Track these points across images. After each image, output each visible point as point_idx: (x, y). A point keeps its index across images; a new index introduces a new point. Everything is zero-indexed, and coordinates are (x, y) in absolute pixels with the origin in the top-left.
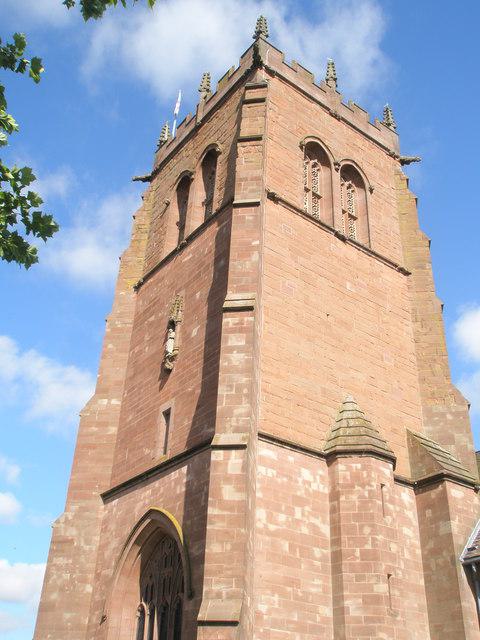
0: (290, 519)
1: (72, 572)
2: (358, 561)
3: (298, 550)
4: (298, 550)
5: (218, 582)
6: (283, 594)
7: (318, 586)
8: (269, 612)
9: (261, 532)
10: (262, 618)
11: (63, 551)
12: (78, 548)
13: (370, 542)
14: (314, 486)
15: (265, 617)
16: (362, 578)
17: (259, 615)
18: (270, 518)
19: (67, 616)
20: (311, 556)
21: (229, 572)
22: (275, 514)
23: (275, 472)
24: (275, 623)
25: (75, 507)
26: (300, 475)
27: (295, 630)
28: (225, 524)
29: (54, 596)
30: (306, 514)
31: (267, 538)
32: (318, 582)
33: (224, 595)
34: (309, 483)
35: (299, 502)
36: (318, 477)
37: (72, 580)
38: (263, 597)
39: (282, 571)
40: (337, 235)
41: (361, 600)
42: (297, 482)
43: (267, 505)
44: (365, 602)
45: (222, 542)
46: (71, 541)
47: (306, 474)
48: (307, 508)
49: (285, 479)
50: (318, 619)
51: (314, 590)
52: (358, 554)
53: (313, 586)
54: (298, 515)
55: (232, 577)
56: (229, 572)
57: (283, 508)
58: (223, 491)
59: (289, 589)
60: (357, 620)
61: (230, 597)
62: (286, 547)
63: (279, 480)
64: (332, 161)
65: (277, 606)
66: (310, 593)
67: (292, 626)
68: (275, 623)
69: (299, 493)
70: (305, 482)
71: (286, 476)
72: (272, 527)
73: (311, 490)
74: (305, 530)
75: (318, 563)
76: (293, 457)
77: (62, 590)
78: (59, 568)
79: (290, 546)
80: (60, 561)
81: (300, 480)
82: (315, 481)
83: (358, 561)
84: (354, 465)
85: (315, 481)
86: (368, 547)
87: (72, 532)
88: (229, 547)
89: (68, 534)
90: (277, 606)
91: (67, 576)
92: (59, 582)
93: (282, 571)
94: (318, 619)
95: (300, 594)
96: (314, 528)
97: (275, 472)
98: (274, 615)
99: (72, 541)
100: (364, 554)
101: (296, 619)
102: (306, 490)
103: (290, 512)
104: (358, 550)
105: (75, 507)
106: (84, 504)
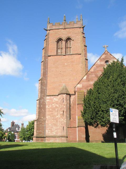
8: (48, 118)
9: (47, 108)
18: (48, 106)
24: (49, 119)
34: (55, 100)
35: (54, 103)
39: (50, 113)
40: (63, 55)
43: (48, 105)
47: (55, 99)
48: (55, 104)
50: (56, 118)
54: (53, 105)
59: (51, 115)
64: (63, 40)
68: (49, 119)
70: (54, 100)
72: (49, 108)
74: (54, 107)
76: (52, 97)
96: (56, 106)
98: (49, 118)
103: (52, 105)
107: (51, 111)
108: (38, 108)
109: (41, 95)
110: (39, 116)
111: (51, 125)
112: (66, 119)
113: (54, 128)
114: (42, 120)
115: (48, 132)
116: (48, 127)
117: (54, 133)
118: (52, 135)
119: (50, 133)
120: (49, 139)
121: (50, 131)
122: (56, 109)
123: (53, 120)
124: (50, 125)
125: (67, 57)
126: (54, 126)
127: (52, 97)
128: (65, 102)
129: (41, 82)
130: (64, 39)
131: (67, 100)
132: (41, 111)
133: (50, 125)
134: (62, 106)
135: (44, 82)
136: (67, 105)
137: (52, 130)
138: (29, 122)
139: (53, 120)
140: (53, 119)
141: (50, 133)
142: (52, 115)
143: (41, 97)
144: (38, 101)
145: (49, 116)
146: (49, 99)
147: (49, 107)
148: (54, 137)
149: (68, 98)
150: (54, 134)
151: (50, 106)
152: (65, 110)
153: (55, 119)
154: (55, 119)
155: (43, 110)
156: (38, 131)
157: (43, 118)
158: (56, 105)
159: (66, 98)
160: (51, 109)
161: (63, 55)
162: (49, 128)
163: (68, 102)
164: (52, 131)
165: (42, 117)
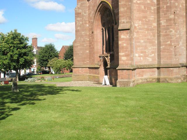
1: (82, 22)
2: (165, 9)
4: (146, 8)
5: (123, 19)
6: (142, 21)
9: (135, 3)
10: (136, 28)
11: (78, 16)
12: (83, 15)
13: (169, 3)
15: (137, 27)
16: (166, 14)
17: (135, 27)
19: (83, 32)
20: (151, 9)
21: (126, 16)
24: (140, 29)
25: (80, 4)
28: (124, 2)
29: (79, 28)
31: (137, 5)
32: (152, 17)
33: (125, 23)
37: (83, 24)
38: (136, 22)
39: (142, 15)
41: (165, 20)
44: (166, 21)
45: (124, 8)
46: (81, 13)
50: (153, 27)
51: (151, 19)
52: (165, 7)
53: (151, 18)
55: (127, 17)
56: (126, 16)
59: (144, 19)
60: (164, 26)
61: (127, 23)
62: (143, 8)
65: (140, 24)
66: (150, 20)
67: (145, 29)
68: (140, 29)
75: (152, 11)
77: (80, 26)
78: (78, 21)
79: (144, 7)
80: (79, 19)
83: (165, 9)
86: (168, 5)
87: (80, 11)
88: (126, 9)
89: (79, 12)
90: (140, 24)
91: (81, 23)
92: (79, 25)
94: (153, 27)
95: (147, 20)
98: (140, 27)
99: (81, 13)
100: (167, 7)
104: (165, 6)
105: (80, 4)
106: (82, 3)
111: (144, 42)
113: (150, 48)
115: (140, 56)
117: (150, 60)
118: (146, 63)
119: (142, 58)
120: (143, 72)
121: (142, 54)
123: (147, 32)
124: (142, 41)
133: (142, 41)
137: (145, 52)
138: (15, 31)
140: (147, 29)
141: (142, 58)
148: (151, 67)
150: (149, 61)
164: (146, 56)
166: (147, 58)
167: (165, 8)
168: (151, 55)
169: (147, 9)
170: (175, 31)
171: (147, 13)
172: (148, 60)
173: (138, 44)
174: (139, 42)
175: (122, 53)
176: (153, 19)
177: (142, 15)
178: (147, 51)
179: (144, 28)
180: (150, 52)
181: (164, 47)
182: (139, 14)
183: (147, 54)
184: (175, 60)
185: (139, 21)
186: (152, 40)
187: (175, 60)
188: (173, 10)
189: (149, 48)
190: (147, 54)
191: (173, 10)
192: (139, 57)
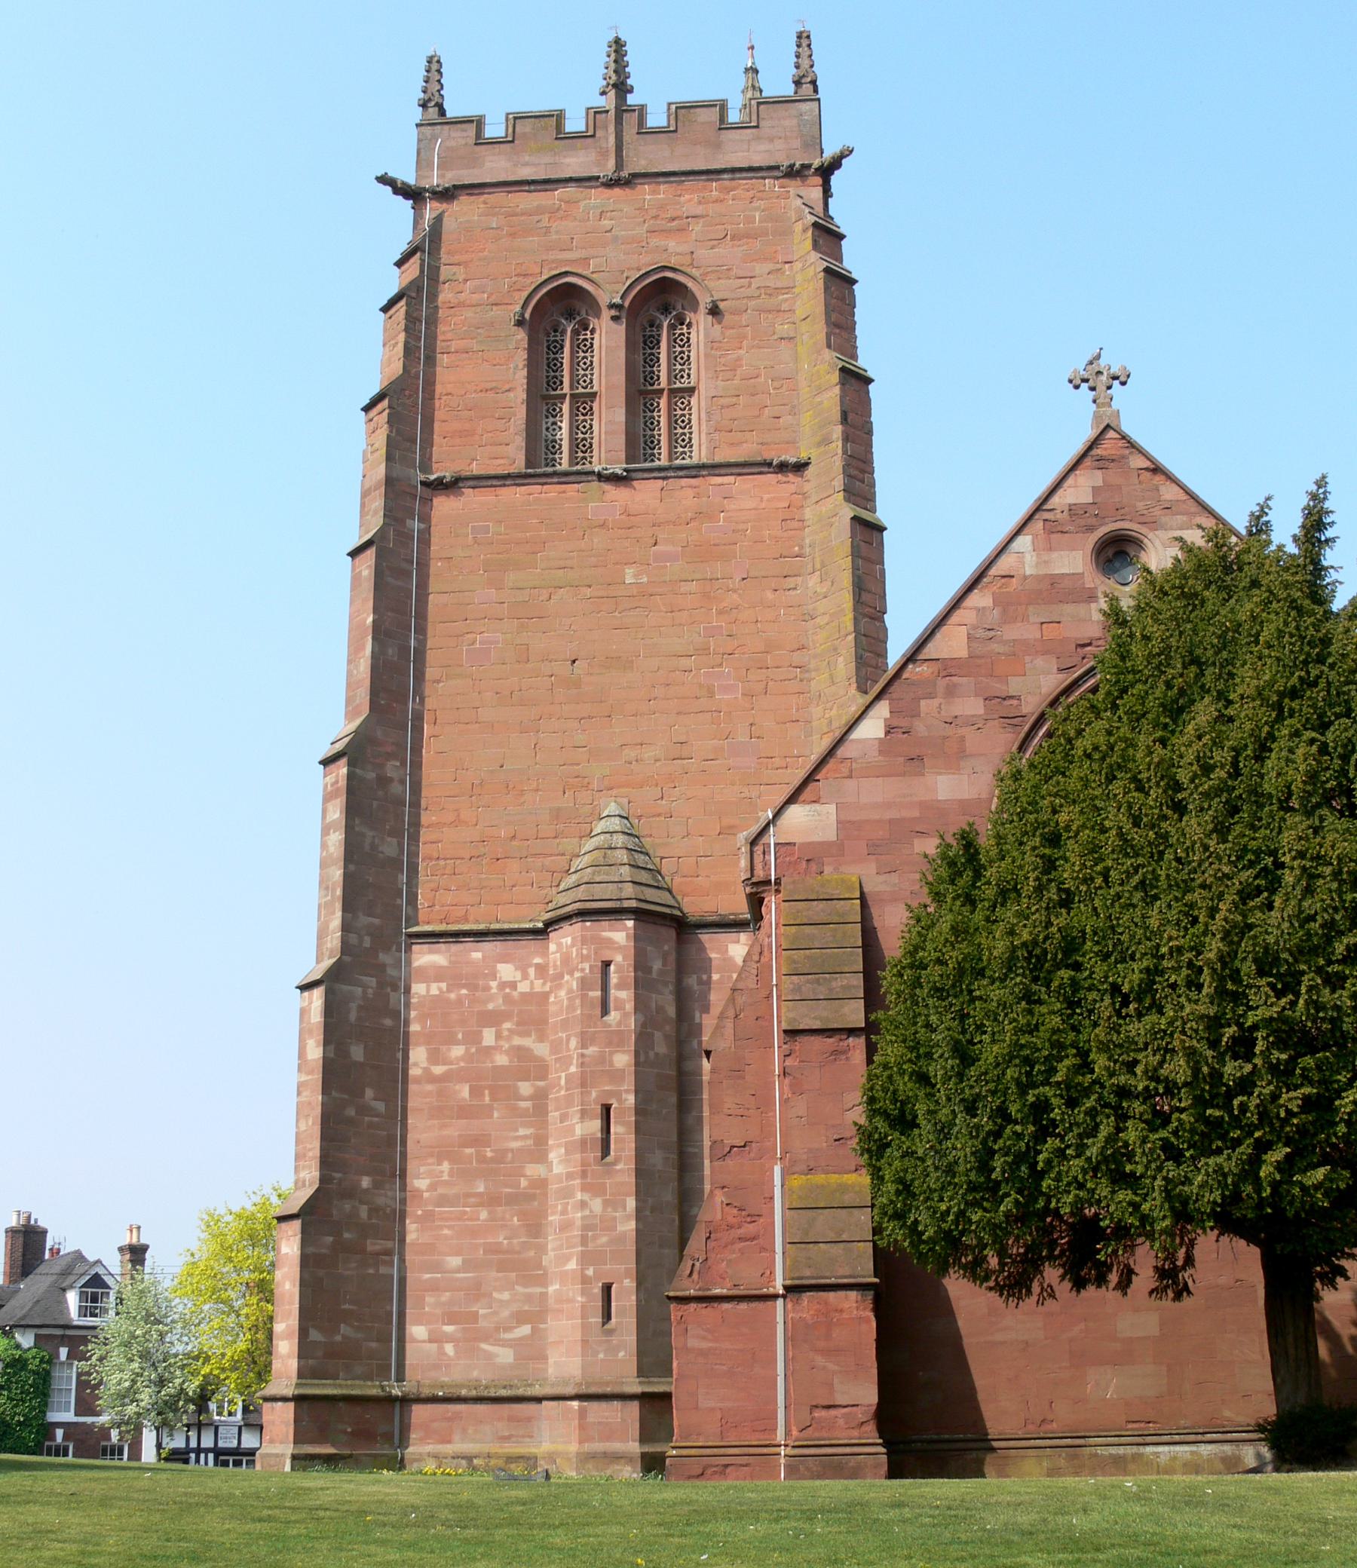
0: (473, 1050)
2: (563, 1093)
3: (487, 1092)
4: (487, 1092)
7: (525, 1137)
8: (432, 1187)
14: (523, 987)
15: (426, 1195)
18: (435, 1057)
22: (444, 1048)
23: (444, 985)
24: (443, 1201)
26: (493, 976)
27: (481, 1205)
30: (506, 1033)
31: (429, 1087)
32: (522, 1132)
34: (513, 985)
35: (492, 1019)
36: (532, 971)
38: (422, 1169)
39: (455, 1129)
40: (601, 477)
41: (563, 1150)
42: (488, 988)
43: (429, 1038)
47: (507, 971)
48: (507, 1025)
49: (464, 991)
50: (524, 1183)
53: (517, 1138)
54: (489, 1037)
57: (460, 1036)
58: (308, 1047)
59: (468, 1151)
63: (453, 996)
65: (445, 1177)
66: (507, 1150)
67: (472, 1200)
68: (443, 1201)
69: (491, 1006)
70: (503, 985)
71: (464, 986)
72: (438, 1070)
73: (515, 994)
74: (502, 1060)
76: (477, 953)
81: (494, 984)
82: (525, 976)
83: (563, 1093)
84: (563, 941)
85: (525, 976)
90: (445, 1177)
93: (455, 1129)
94: (524, 1183)
95: (489, 1154)
96: (521, 1053)
97: (444, 985)
98: (440, 1191)
101: (481, 1189)
102: (507, 999)
103: (473, 1038)
107: (464, 1112)
108: (317, 1077)
109: (346, 927)
110: (326, 1162)
111: (467, 1266)
112: (631, 1203)
113: (506, 1296)
114: (364, 1212)
115: (435, 1338)
116: (435, 1288)
117: (505, 1356)
120: (457, 1417)
121: (449, 1329)
122: (525, 1088)
123: (484, 1215)
124: (455, 1261)
125: (646, 493)
126: (493, 1274)
127: (477, 955)
128: (630, 1007)
129: (350, 777)
130: (609, 292)
131: (643, 983)
132: (351, 1112)
133: (455, 1261)
134: (592, 1050)
135: (383, 781)
136: (643, 1039)
137: (474, 1317)
139: (484, 1215)
140: (491, 1201)
141: (449, 1349)
142: (482, 1159)
143: (346, 947)
144: (317, 996)
145: (446, 1166)
146: (437, 974)
147: (446, 1062)
148: (503, 1393)
149: (657, 966)
150: (499, 1360)
151: (458, 1051)
152: (631, 1099)
153: (512, 1200)
154: (512, 1200)
155: (369, 1093)
156: (315, 1335)
157: (377, 1185)
158: (517, 1041)
159: (641, 965)
160: (464, 1091)
161: (601, 477)
162: (446, 1296)
163: (660, 1009)
164: (473, 1336)
165: (366, 1182)
166: (484, 1346)
167: (561, 1088)
168: (508, 1329)
169: (487, 1099)
170: (606, 1203)
171: (492, 1117)
172: (489, 1356)
173: (428, 1276)
174: (436, 1267)
175: (282, 1322)
176: (530, 1142)
177: (457, 1133)
178: (481, 1312)
179: (468, 1195)
180: (505, 1313)
181: (558, 1287)
182: (443, 1126)
183: (482, 1323)
184: (601, 1356)
185: (439, 1164)
186: (519, 1253)
187: (601, 1356)
188: (594, 1094)
189: (495, 1295)
190: (482, 1323)
191: (594, 1094)
192: (430, 1341)
